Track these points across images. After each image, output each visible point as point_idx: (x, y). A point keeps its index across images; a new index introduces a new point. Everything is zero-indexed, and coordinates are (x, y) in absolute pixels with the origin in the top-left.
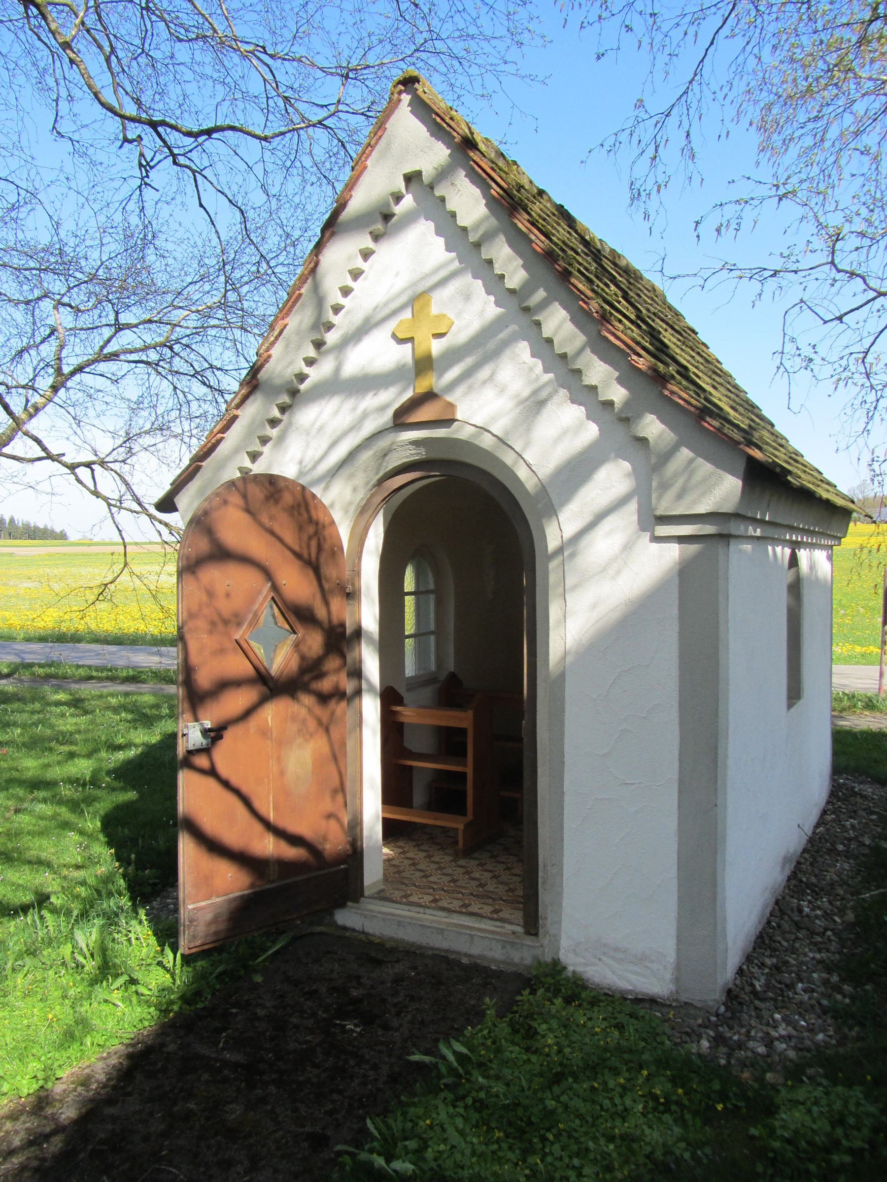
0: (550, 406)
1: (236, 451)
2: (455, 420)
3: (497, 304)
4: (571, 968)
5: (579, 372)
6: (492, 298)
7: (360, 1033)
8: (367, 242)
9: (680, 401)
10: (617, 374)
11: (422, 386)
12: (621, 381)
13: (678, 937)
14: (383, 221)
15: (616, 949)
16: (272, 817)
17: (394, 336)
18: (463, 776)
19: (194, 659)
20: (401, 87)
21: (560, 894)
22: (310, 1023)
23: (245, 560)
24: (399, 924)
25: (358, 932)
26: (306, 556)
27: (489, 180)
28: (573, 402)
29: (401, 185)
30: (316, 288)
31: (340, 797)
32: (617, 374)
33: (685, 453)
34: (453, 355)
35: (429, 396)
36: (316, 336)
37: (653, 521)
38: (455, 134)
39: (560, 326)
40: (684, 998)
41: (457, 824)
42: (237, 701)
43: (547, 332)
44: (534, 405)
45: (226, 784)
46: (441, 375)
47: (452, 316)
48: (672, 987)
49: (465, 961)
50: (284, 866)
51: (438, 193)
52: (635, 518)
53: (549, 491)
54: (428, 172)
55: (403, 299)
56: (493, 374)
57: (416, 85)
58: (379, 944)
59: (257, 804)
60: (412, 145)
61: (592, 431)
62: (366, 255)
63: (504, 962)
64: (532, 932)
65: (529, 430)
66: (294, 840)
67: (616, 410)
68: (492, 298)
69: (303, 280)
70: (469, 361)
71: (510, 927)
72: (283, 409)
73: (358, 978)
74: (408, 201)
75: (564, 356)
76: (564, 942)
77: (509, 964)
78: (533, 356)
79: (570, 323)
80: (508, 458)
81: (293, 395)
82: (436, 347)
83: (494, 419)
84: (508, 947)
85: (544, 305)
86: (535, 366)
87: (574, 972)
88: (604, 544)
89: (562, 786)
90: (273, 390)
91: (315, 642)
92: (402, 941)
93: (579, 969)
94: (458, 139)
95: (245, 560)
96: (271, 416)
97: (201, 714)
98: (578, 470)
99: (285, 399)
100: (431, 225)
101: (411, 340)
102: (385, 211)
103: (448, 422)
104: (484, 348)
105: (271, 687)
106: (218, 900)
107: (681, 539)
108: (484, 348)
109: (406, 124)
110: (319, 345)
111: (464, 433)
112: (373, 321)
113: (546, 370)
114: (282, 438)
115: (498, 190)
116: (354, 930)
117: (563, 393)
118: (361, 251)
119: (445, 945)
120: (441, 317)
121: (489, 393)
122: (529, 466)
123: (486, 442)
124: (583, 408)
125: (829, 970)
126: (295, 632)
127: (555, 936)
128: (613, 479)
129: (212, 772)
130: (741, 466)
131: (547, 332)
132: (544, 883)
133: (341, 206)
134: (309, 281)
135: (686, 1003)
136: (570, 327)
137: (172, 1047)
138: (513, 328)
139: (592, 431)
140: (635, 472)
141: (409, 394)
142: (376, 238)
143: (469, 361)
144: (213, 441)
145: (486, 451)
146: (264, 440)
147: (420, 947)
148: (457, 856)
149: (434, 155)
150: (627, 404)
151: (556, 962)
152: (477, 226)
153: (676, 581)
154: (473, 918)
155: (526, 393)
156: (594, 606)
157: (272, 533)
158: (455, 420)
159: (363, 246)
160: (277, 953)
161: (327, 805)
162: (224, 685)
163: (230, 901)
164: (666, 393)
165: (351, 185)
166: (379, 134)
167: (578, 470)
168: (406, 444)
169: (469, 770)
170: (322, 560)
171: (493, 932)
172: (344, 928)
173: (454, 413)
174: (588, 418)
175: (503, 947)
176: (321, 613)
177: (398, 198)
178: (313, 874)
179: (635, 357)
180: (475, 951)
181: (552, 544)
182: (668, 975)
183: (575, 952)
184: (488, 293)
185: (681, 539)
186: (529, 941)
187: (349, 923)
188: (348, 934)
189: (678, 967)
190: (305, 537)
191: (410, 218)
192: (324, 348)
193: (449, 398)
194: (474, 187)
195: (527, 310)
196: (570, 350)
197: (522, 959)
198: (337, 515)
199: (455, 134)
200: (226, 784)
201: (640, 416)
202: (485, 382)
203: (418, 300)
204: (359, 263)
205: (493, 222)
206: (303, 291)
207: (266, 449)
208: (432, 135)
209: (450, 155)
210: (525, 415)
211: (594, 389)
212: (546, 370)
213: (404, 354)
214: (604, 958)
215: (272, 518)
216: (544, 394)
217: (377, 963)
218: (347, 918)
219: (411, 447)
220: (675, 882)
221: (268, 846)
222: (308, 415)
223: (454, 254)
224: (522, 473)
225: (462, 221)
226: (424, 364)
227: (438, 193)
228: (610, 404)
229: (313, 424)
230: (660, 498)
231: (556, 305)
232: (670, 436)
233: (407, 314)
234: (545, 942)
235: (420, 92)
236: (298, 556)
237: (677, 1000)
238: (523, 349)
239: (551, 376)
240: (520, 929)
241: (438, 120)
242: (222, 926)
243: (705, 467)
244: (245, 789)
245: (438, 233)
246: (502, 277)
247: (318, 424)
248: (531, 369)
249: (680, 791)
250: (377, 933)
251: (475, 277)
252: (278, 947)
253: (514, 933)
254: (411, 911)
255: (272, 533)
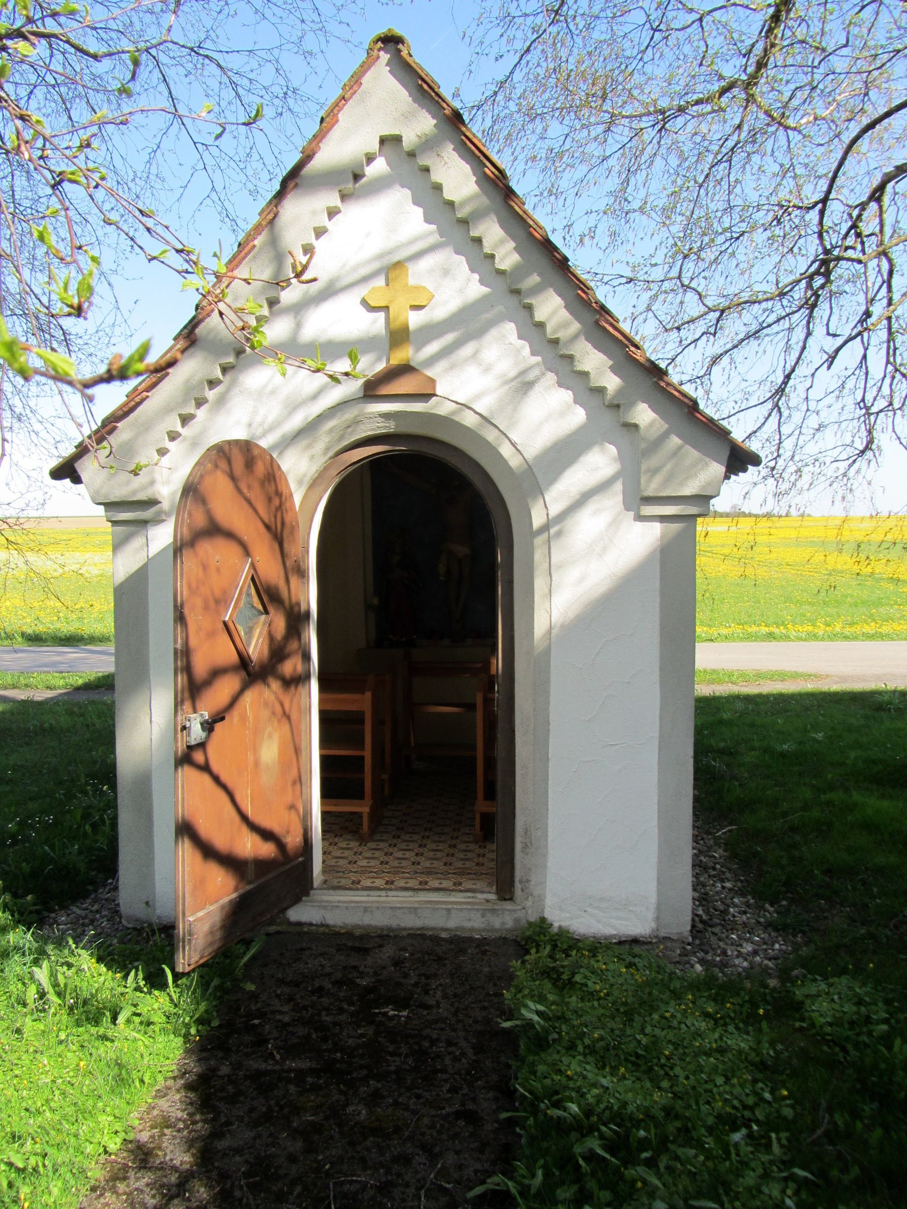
0: (537, 388)
1: (167, 410)
2: (434, 395)
3: (482, 282)
4: (556, 925)
5: (571, 358)
6: (476, 277)
7: (407, 1017)
8: (334, 200)
9: (676, 394)
10: (611, 363)
11: (398, 357)
12: (613, 369)
13: (658, 879)
14: (351, 181)
15: (602, 899)
16: (249, 812)
17: (364, 303)
18: (362, 758)
19: (193, 642)
20: (380, 44)
21: (545, 856)
22: (343, 1017)
23: (230, 535)
24: (366, 910)
25: (316, 925)
26: (273, 527)
27: (482, 158)
28: (560, 385)
29: (375, 146)
30: (274, 241)
31: (298, 786)
32: (611, 363)
33: (675, 441)
34: (432, 331)
35: (405, 369)
36: (271, 294)
37: (639, 502)
38: (445, 105)
39: (554, 313)
40: (662, 934)
41: (363, 808)
42: (226, 687)
43: (539, 316)
44: (523, 385)
45: (217, 779)
46: (418, 349)
47: (430, 288)
48: (653, 925)
49: (444, 935)
50: (262, 865)
51: (423, 161)
52: (620, 498)
53: (535, 470)
54: (410, 139)
55: (376, 265)
56: (475, 355)
57: (400, 46)
58: (346, 933)
59: (238, 798)
60: (384, 105)
61: (579, 416)
62: (332, 213)
63: (484, 930)
64: (507, 897)
65: (515, 409)
66: (267, 835)
67: (608, 397)
68: (476, 277)
69: (258, 229)
70: (449, 338)
71: (481, 896)
72: (225, 370)
73: (355, 968)
74: (379, 167)
75: (555, 342)
76: (549, 901)
77: (488, 931)
78: (520, 337)
79: (564, 310)
80: (490, 435)
81: (240, 353)
82: (414, 320)
83: (478, 397)
84: (488, 915)
85: (537, 290)
86: (523, 347)
87: (560, 927)
88: (589, 524)
89: (548, 753)
90: (216, 348)
91: (280, 624)
92: (370, 926)
93: (564, 924)
94: (448, 111)
95: (230, 535)
96: (212, 377)
97: (199, 705)
98: (565, 453)
99: (231, 359)
100: (407, 193)
101: (386, 309)
102: (358, 172)
103: (426, 397)
104: (468, 324)
105: (251, 672)
106: (212, 908)
107: (663, 519)
108: (468, 324)
109: (383, 82)
110: (273, 303)
111: (440, 407)
112: (339, 285)
113: (533, 353)
114: (222, 401)
115: (494, 170)
116: (311, 924)
117: (551, 377)
118: (328, 209)
119: (419, 923)
120: (418, 288)
121: (472, 371)
122: (514, 445)
123: (469, 420)
124: (570, 393)
125: (743, 895)
126: (266, 612)
127: (539, 896)
128: (599, 463)
129: (206, 768)
130: (726, 454)
131: (539, 316)
132: (525, 846)
133: (307, 157)
134: (264, 233)
135: (664, 938)
136: (564, 314)
137: (225, 1070)
138: (500, 308)
139: (579, 416)
140: (621, 457)
141: (381, 366)
142: (344, 197)
143: (449, 338)
144: (137, 399)
145: (468, 428)
146: (200, 402)
147: (390, 929)
148: (363, 840)
149: (421, 125)
150: (620, 392)
151: (543, 920)
152: (464, 203)
153: (658, 556)
154: (442, 893)
155: (513, 373)
156: (582, 580)
157: (249, 502)
158: (434, 395)
159: (332, 204)
160: (253, 958)
161: (289, 798)
162: (216, 673)
163: (223, 907)
164: (663, 384)
165: (319, 137)
166: (355, 88)
167: (565, 453)
168: (377, 416)
169: (367, 754)
170: (285, 535)
171: (469, 903)
172: (299, 924)
173: (434, 388)
174: (575, 402)
175: (483, 916)
176: (284, 594)
177: (370, 159)
178: (282, 869)
179: (632, 349)
180: (451, 924)
181: (538, 519)
182: (651, 915)
183: (561, 909)
184: (472, 270)
185: (663, 519)
186: (508, 905)
187: (304, 919)
188: (306, 929)
189: (659, 908)
190: (273, 509)
191: (380, 185)
192: (276, 307)
193: (429, 373)
194: (463, 163)
195: (517, 292)
196: (562, 335)
197: (503, 923)
198: (293, 486)
199: (445, 105)
200: (217, 779)
201: (632, 404)
202: (466, 360)
203: (392, 269)
204: (324, 220)
205: (485, 201)
206: (256, 242)
207: (201, 414)
208: (414, 101)
209: (435, 126)
210: (499, 395)
211: (585, 374)
212: (533, 353)
213: (376, 324)
214: (589, 910)
215: (249, 487)
216: (531, 376)
217: (364, 951)
218: (299, 914)
219: (380, 420)
220: (656, 830)
221: (249, 846)
222: (257, 377)
223: (433, 227)
224: (506, 451)
225: (448, 195)
226: (398, 336)
227: (423, 161)
228: (601, 390)
229: (265, 387)
230: (649, 481)
231: (551, 290)
232: (662, 426)
233: (380, 282)
234: (529, 903)
235: (404, 53)
236: (268, 527)
237: (657, 937)
238: (510, 329)
239: (538, 359)
240: (492, 897)
241: (425, 86)
242: (218, 935)
243: (693, 454)
244: (230, 784)
245: (416, 203)
246: (492, 257)
247: (269, 388)
248: (518, 351)
249: (660, 749)
250: (339, 923)
251: (457, 252)
252: (252, 952)
253: (488, 901)
254: (375, 899)
255: (249, 502)
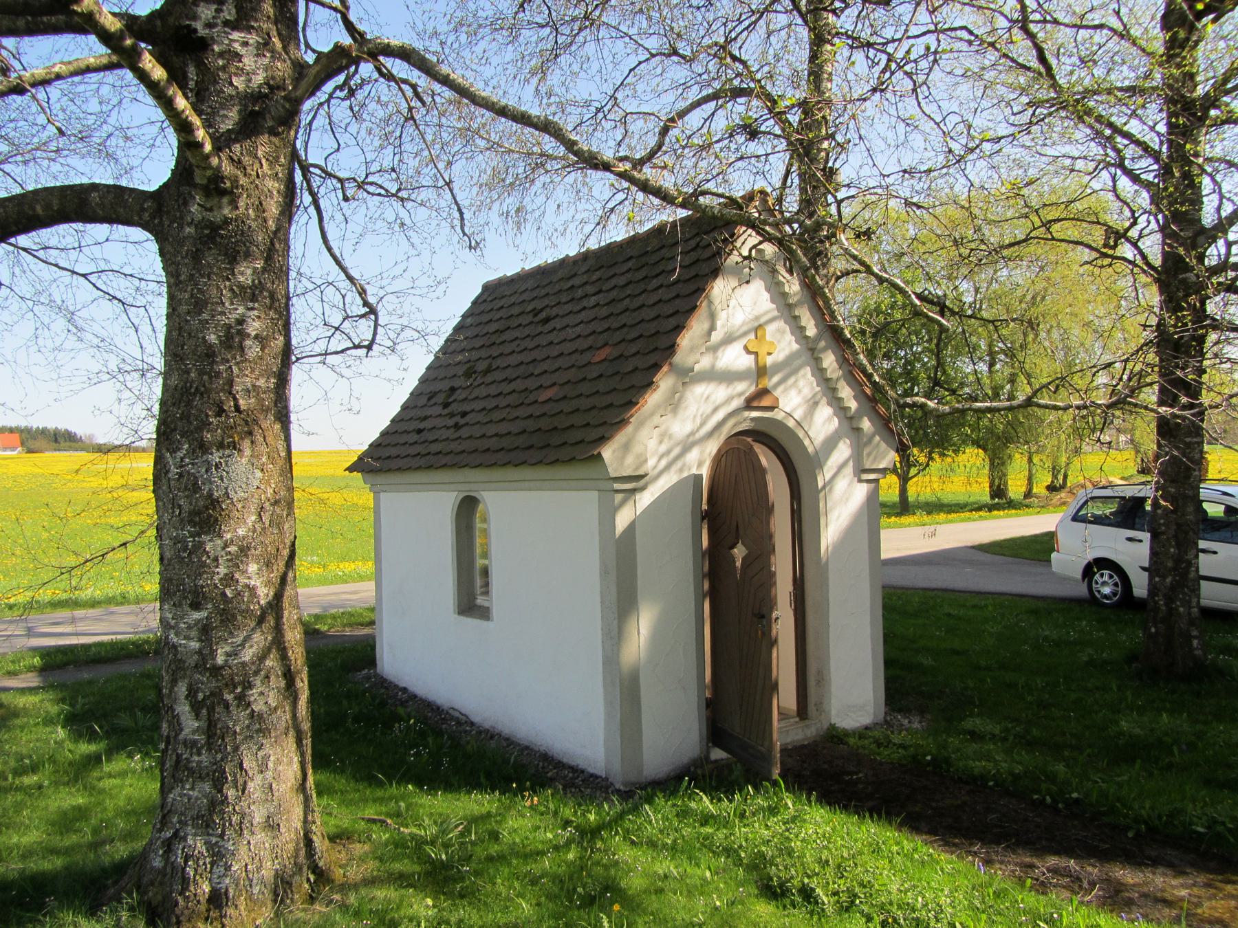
12: (855, 397)
17: (746, 348)
34: (778, 367)
44: (813, 405)
76: (833, 712)
80: (801, 434)
82: (769, 361)
83: (795, 409)
85: (824, 350)
88: (841, 485)
101: (756, 354)
103: (771, 408)
104: (789, 367)
108: (789, 367)
111: (778, 415)
123: (791, 423)
128: (843, 451)
138: (803, 358)
150: (857, 410)
167: (831, 443)
185: (868, 481)
213: (747, 362)
224: (806, 442)
226: (761, 371)
232: (872, 429)
243: (883, 445)
